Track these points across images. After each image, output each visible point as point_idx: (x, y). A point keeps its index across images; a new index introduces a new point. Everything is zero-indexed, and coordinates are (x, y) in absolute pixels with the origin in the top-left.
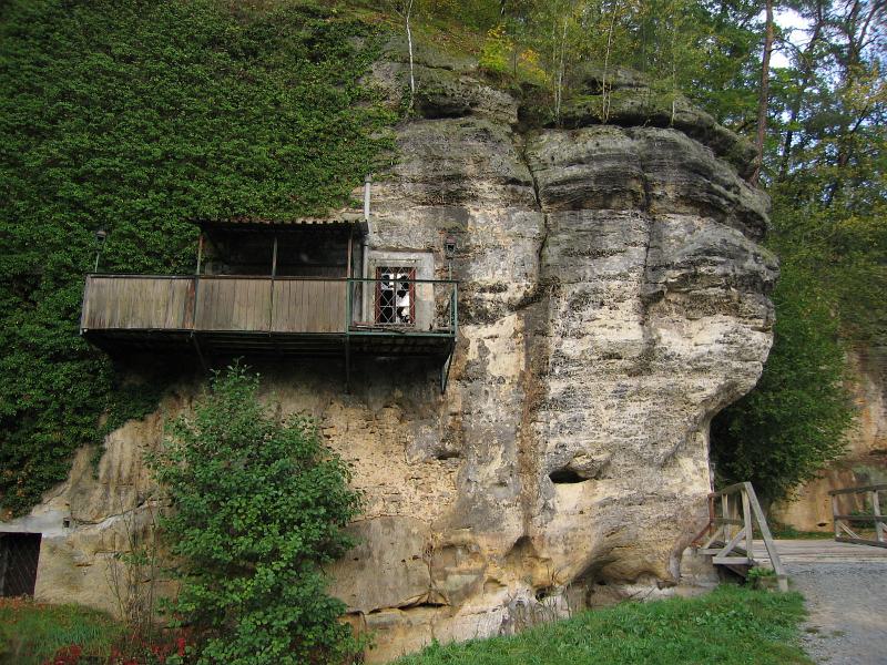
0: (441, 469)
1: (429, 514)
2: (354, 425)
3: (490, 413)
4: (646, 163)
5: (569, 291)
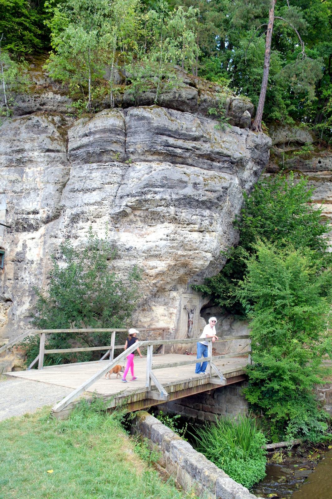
3: (27, 279)
4: (125, 131)
5: (69, 212)
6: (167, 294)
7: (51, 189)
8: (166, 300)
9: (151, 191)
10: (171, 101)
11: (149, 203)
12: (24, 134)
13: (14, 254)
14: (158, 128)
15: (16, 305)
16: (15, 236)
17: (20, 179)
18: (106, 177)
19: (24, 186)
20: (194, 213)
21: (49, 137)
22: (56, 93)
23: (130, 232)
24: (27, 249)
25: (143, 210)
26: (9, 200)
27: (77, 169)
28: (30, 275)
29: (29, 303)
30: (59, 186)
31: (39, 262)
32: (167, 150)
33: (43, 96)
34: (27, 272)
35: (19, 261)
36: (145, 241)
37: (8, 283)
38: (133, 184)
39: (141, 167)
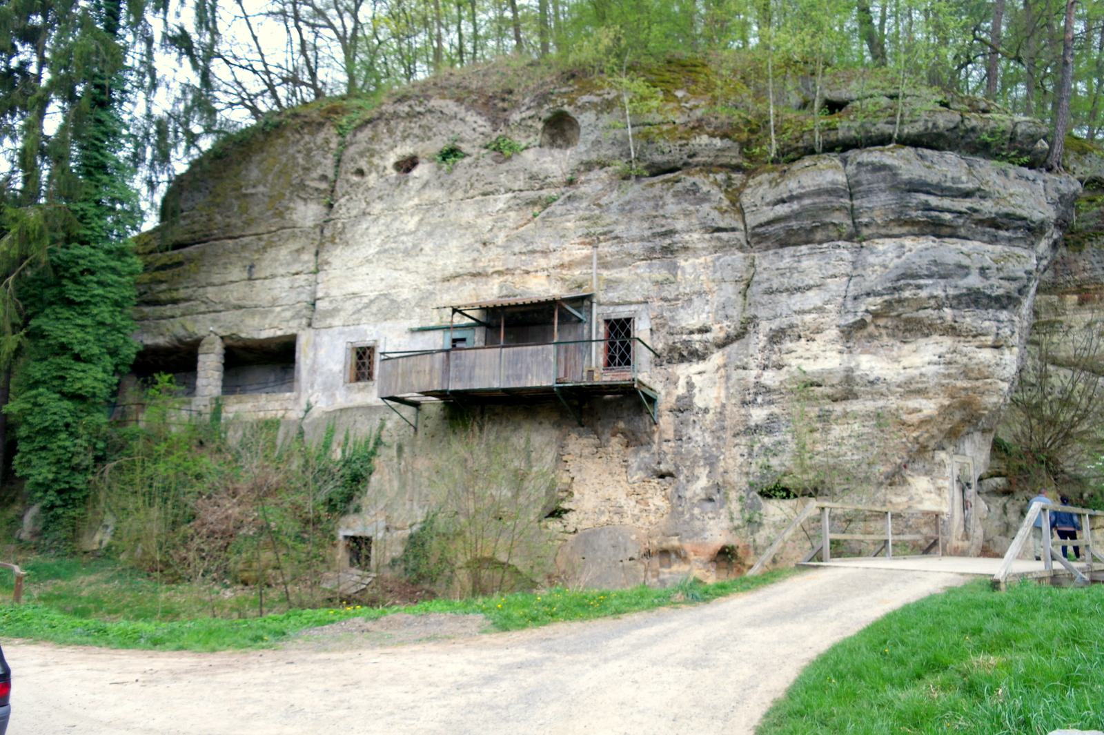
0: (657, 486)
1: (647, 524)
2: (586, 452)
3: (699, 439)
4: (851, 191)
5: (765, 327)
6: (928, 455)
7: (730, 290)
8: (928, 467)
9: (910, 285)
10: (920, 135)
11: (906, 304)
12: (672, 207)
13: (673, 400)
14: (910, 182)
15: (685, 482)
16: (670, 370)
17: (672, 278)
18: (828, 266)
19: (681, 290)
20: (985, 317)
21: (716, 208)
22: (712, 136)
23: (871, 353)
24: (696, 391)
25: (892, 317)
26: (655, 314)
27: (771, 257)
28: (704, 431)
29: (707, 476)
30: (742, 286)
31: (719, 410)
32: (927, 217)
33: (693, 142)
34: (698, 427)
35: (680, 411)
36: (901, 367)
37: (665, 447)
38: (875, 276)
39: (885, 247)
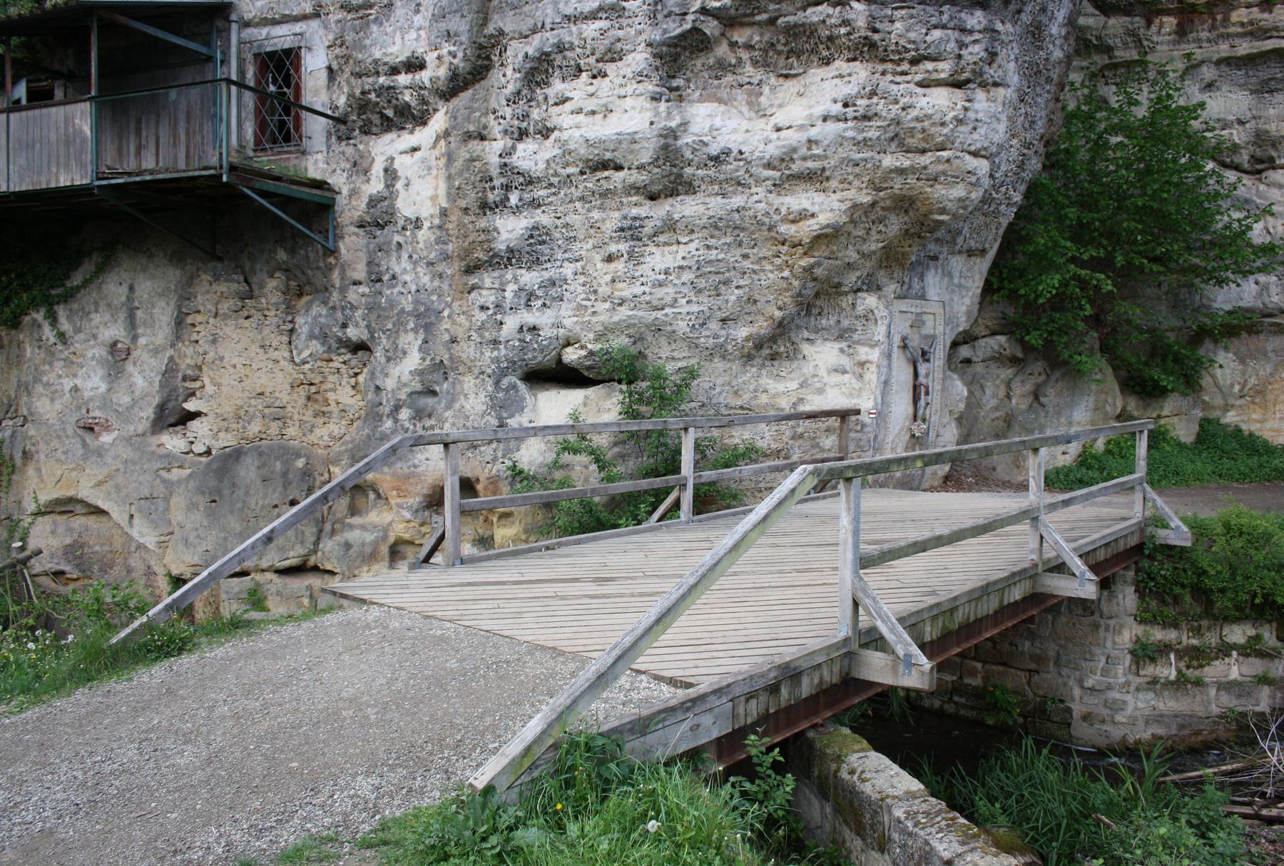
0: (344, 368)
1: (326, 438)
2: (225, 307)
3: (407, 278)
5: (517, 53)
6: (846, 302)
8: (846, 323)
13: (362, 204)
15: (383, 360)
16: (361, 147)
20: (934, 21)
23: (720, 101)
24: (399, 185)
25: (759, 24)
28: (415, 263)
29: (420, 350)
31: (437, 221)
34: (405, 256)
35: (378, 225)
